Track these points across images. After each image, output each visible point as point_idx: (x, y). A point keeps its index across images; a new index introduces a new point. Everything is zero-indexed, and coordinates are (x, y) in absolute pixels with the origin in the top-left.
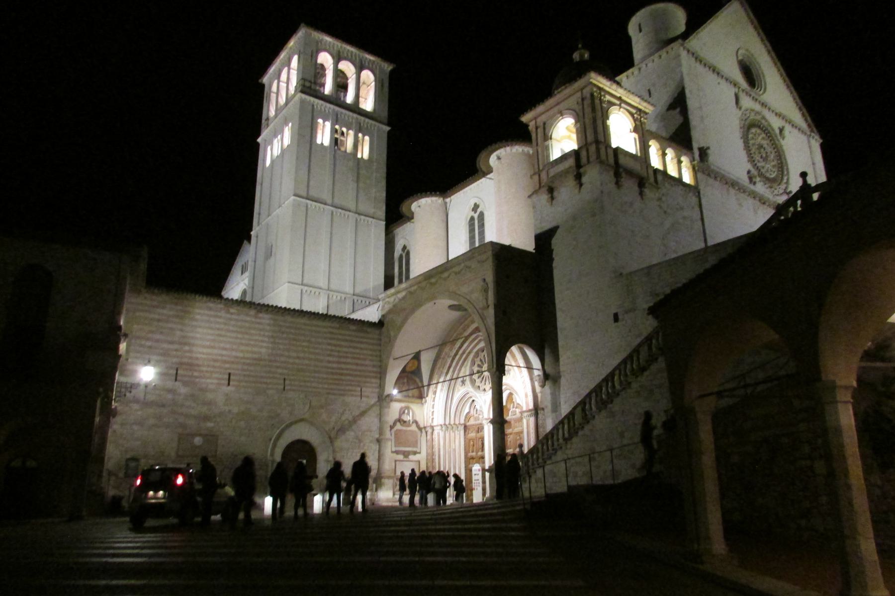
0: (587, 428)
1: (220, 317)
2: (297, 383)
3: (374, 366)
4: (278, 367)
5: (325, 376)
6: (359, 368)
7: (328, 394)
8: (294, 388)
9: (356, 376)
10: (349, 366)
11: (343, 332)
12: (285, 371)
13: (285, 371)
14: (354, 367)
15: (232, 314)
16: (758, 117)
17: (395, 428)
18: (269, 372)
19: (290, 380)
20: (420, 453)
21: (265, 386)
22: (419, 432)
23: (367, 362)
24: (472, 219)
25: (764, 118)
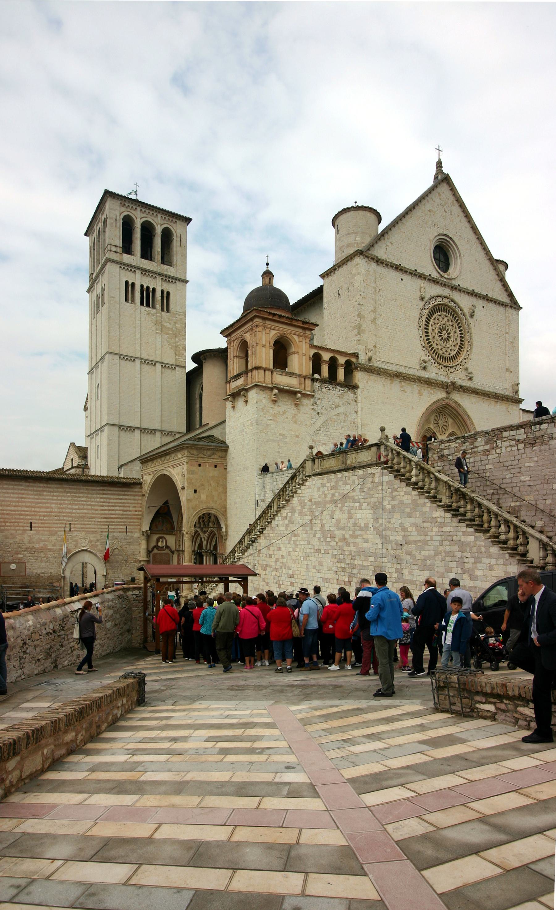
1: (22, 485)
2: (79, 526)
3: (136, 511)
4: (64, 516)
5: (99, 520)
7: (101, 532)
8: (76, 529)
9: (122, 518)
10: (117, 512)
11: (112, 489)
12: (70, 519)
13: (70, 519)
14: (121, 512)
15: (29, 482)
19: (74, 524)
21: (56, 529)
22: (171, 554)
23: (131, 509)
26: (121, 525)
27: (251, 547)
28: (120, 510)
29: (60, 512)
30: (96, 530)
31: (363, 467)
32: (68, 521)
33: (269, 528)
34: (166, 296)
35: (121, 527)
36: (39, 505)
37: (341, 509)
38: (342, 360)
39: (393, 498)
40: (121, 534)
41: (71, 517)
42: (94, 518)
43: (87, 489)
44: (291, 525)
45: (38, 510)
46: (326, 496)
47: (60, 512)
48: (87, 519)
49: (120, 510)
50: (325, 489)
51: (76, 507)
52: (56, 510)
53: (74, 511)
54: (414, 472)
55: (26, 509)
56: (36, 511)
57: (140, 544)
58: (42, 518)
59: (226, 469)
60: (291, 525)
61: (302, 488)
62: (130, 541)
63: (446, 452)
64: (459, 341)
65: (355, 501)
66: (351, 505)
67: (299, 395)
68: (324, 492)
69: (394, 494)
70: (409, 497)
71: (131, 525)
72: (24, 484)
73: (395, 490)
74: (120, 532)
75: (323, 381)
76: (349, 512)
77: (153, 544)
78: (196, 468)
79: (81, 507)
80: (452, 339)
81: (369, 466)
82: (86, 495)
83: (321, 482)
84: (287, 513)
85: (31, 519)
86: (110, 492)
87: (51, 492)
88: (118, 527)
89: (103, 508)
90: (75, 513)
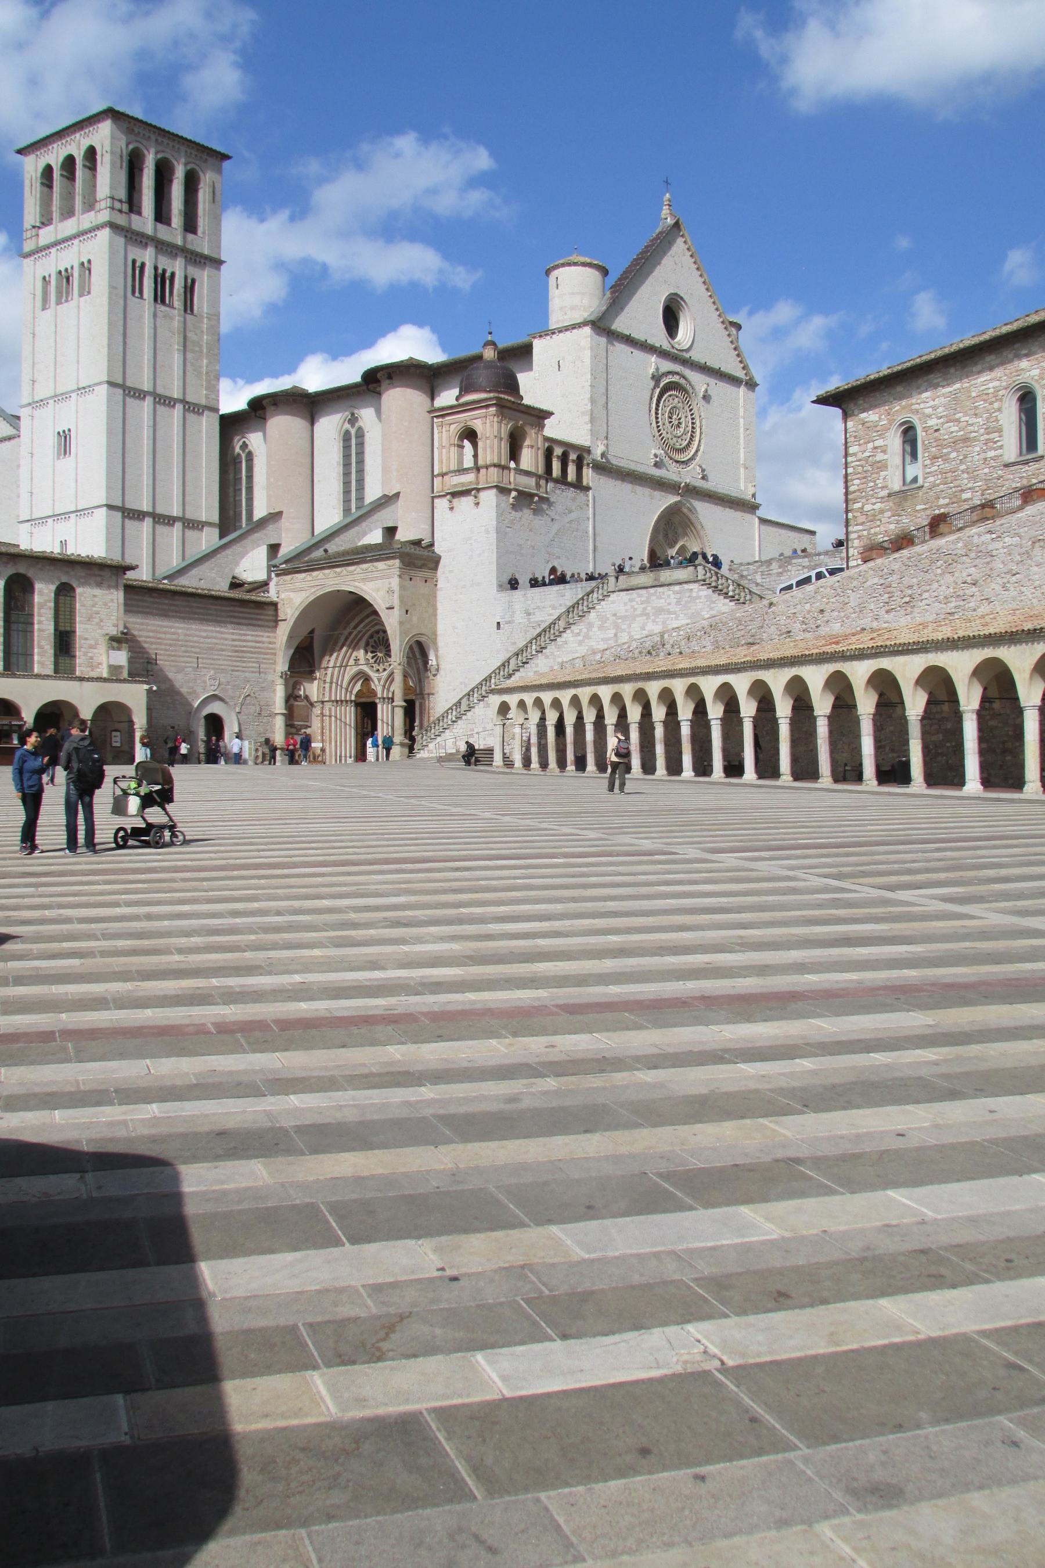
0: (468, 714)
4: (192, 647)
5: (230, 654)
6: (258, 645)
7: (233, 671)
9: (255, 653)
12: (198, 650)
14: (253, 644)
16: (675, 378)
17: (290, 703)
18: (186, 652)
19: (203, 658)
20: (310, 727)
23: (264, 639)
24: (347, 433)
25: (684, 377)
26: (254, 662)
27: (521, 670)
28: (252, 641)
29: (187, 641)
30: (226, 667)
31: (680, 583)
32: (196, 653)
33: (553, 647)
34: (189, 289)
35: (254, 665)
36: (164, 629)
37: (654, 621)
38: (573, 456)
39: (712, 609)
40: (254, 675)
41: (199, 648)
42: (223, 650)
43: (216, 610)
44: (586, 641)
45: (163, 636)
46: (635, 610)
47: (187, 641)
48: (216, 652)
49: (252, 641)
50: (634, 603)
51: (204, 634)
52: (182, 637)
53: (202, 640)
54: (731, 588)
55: (151, 634)
56: (159, 638)
57: (275, 690)
58: (167, 647)
59: (436, 585)
60: (586, 641)
61: (603, 603)
62: (263, 685)
63: (745, 573)
64: (690, 428)
65: (669, 612)
66: (666, 616)
67: (536, 498)
68: (632, 607)
69: (712, 605)
70: (727, 607)
71: (266, 663)
72: (149, 599)
73: (714, 602)
74: (253, 672)
75: (556, 481)
76: (664, 623)
77: (290, 691)
78: (407, 583)
79: (210, 634)
80: (683, 425)
81: (686, 583)
82: (214, 618)
83: (629, 597)
84: (581, 630)
85: (157, 649)
86: (241, 615)
87: (176, 612)
88: (250, 664)
89: (234, 637)
90: (202, 643)
